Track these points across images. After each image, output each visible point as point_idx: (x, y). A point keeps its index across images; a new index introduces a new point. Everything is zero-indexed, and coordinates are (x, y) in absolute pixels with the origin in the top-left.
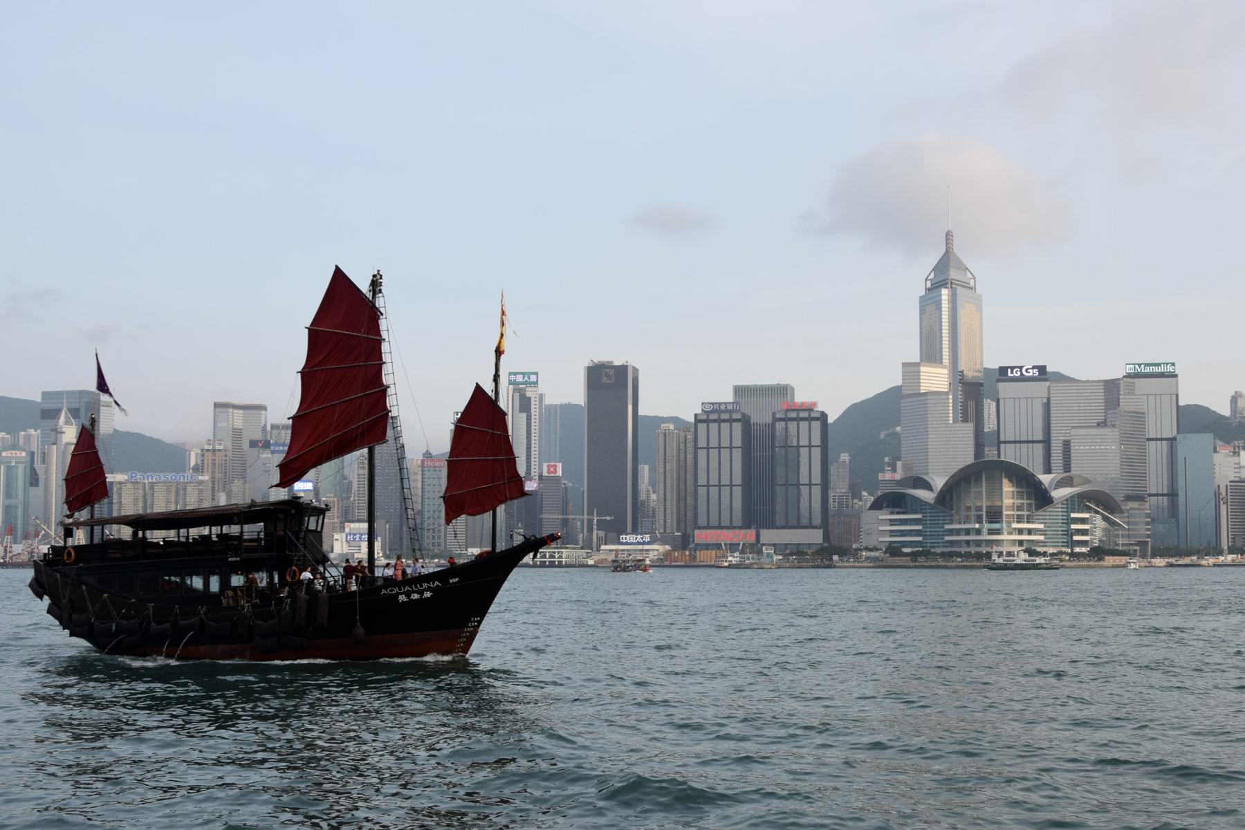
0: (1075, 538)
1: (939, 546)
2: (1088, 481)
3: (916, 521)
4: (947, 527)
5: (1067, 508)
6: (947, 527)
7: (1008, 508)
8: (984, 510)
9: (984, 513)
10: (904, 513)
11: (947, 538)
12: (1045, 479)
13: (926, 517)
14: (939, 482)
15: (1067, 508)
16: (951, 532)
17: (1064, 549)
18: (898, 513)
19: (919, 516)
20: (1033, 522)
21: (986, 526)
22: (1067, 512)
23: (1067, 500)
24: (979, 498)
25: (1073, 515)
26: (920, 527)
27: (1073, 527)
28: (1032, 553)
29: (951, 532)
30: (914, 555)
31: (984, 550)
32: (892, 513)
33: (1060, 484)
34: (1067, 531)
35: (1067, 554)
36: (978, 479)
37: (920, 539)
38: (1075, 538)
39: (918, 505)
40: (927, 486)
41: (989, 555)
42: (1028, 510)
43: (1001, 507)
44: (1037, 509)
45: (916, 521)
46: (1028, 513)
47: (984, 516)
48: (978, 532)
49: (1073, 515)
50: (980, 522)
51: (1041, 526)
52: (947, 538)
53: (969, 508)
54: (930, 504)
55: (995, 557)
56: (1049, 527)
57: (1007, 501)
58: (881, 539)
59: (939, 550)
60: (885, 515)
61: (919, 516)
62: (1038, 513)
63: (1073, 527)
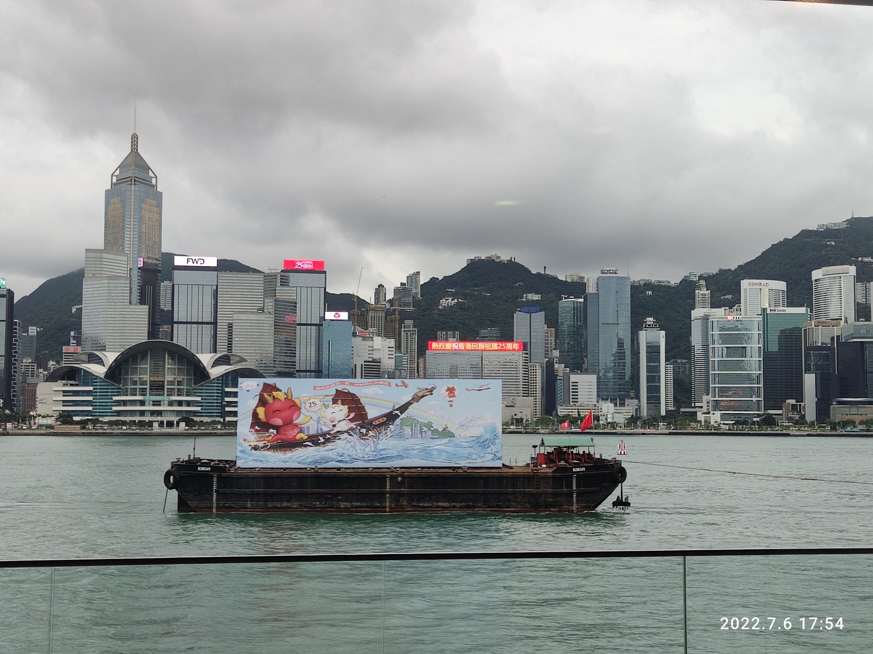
0: (227, 409)
1: (107, 416)
2: (242, 360)
3: (87, 393)
4: (115, 398)
5: (222, 383)
6: (115, 398)
7: (171, 383)
8: (148, 384)
9: (148, 387)
10: (77, 385)
11: (114, 408)
12: (206, 359)
13: (96, 389)
14: (110, 357)
15: (222, 383)
16: (119, 403)
17: (217, 419)
18: (71, 385)
19: (91, 388)
20: (191, 396)
21: (149, 398)
22: (222, 387)
23: (222, 376)
24: (144, 373)
25: (227, 390)
26: (91, 398)
27: (227, 399)
28: (189, 423)
29: (119, 403)
30: (83, 423)
31: (147, 418)
32: (64, 385)
33: (216, 363)
34: (221, 403)
35: (219, 422)
36: (144, 357)
37: (90, 408)
38: (227, 409)
39: (89, 378)
40: (100, 362)
41: (150, 424)
42: (187, 385)
43: (163, 382)
44: (195, 384)
45: (87, 393)
46: (187, 387)
47: (148, 390)
48: (142, 403)
49: (227, 390)
50: (143, 392)
51: (199, 399)
52: (114, 408)
53: (135, 383)
54: (100, 378)
55: (156, 425)
56: (205, 399)
57: (169, 377)
58: (54, 409)
59: (106, 419)
60: (59, 386)
61: (91, 388)
62: (196, 387)
63: (227, 399)
